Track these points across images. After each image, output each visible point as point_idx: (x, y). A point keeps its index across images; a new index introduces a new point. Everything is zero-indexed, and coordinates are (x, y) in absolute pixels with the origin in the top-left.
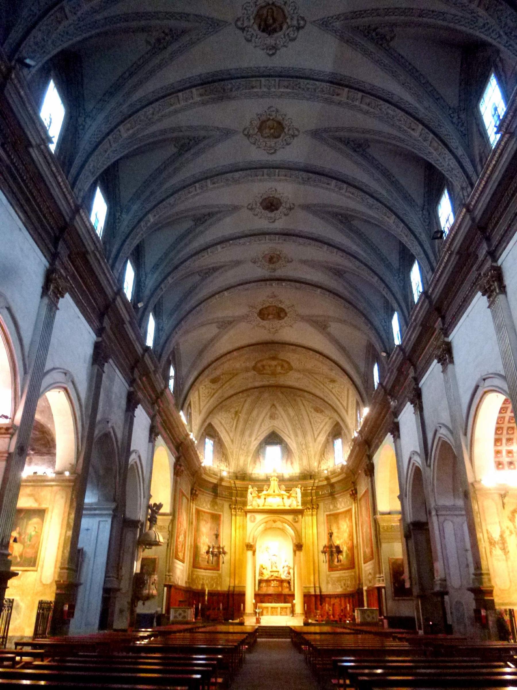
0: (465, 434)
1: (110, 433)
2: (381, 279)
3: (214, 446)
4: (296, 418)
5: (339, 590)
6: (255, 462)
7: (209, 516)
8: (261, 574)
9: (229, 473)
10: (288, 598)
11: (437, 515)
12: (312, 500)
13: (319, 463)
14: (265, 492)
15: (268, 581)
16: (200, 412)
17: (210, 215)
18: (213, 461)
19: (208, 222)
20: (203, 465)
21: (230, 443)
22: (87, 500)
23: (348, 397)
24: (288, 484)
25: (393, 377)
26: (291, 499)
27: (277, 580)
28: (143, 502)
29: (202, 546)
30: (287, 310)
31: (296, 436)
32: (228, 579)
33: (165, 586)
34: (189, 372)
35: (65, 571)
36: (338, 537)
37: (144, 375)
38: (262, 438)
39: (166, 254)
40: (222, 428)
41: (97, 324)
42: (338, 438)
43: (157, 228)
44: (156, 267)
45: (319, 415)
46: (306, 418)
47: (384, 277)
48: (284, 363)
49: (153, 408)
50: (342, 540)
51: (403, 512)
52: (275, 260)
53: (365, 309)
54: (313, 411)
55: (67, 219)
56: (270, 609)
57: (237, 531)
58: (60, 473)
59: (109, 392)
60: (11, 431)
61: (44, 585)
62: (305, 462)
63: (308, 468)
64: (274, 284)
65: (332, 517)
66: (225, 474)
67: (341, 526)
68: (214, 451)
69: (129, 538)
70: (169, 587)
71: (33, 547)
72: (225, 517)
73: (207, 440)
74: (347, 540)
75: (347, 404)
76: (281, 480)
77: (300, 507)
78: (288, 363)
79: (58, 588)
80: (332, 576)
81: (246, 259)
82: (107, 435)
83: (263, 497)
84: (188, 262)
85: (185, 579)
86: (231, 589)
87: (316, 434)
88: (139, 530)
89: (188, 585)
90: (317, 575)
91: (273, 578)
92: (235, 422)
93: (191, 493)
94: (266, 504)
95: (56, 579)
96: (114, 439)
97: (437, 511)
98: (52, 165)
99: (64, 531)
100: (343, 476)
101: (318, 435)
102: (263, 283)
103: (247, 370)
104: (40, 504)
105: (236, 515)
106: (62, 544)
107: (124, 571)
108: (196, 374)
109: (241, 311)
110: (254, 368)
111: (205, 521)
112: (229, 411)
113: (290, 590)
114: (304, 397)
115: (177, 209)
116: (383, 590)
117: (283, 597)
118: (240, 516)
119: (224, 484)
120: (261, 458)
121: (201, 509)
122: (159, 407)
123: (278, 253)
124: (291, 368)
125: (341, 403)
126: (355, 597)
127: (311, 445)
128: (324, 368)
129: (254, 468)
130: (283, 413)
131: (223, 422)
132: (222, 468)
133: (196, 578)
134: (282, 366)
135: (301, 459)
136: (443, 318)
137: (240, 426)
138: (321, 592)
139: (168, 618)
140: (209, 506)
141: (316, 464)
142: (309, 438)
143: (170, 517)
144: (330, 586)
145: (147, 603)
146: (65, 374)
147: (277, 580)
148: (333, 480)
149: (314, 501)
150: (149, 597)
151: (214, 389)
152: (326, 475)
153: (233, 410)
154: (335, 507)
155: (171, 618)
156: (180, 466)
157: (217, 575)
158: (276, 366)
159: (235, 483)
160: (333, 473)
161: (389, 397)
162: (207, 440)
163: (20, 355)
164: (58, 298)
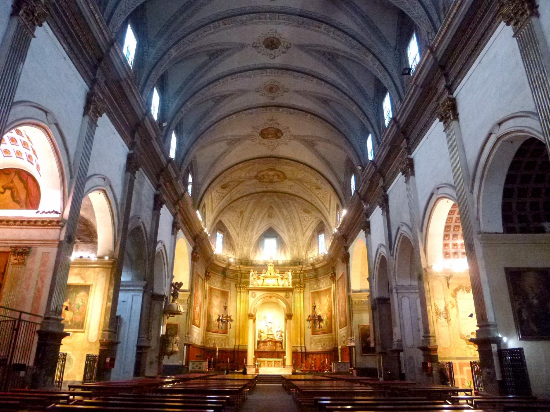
0: (421, 231)
1: (140, 227)
2: (359, 106)
3: (223, 238)
4: (289, 217)
5: (320, 349)
6: (256, 252)
8: (260, 336)
9: (235, 259)
10: (280, 354)
11: (397, 293)
12: (300, 281)
13: (307, 253)
14: (263, 275)
15: (265, 342)
16: (213, 211)
17: (222, 51)
18: (223, 250)
19: (219, 58)
20: (214, 253)
21: (236, 235)
22: (123, 279)
23: (330, 201)
24: (281, 268)
25: (367, 186)
26: (284, 280)
27: (272, 341)
28: (167, 281)
29: (213, 315)
30: (283, 131)
31: (289, 231)
32: (234, 340)
33: (185, 345)
34: (204, 179)
35: (107, 333)
36: (320, 309)
37: (167, 182)
38: (261, 233)
39: (185, 84)
41: (129, 139)
42: (321, 234)
43: (178, 61)
44: (178, 92)
45: (307, 215)
46: (296, 216)
47: (362, 106)
48: (280, 174)
49: (175, 207)
50: (323, 312)
51: (371, 291)
52: (274, 90)
53: (345, 131)
54: (302, 212)
55: (104, 51)
56: (266, 362)
57: (241, 304)
58: (101, 258)
59: (139, 194)
60: (61, 223)
61: (90, 343)
62: (295, 252)
63: (297, 257)
64: (273, 109)
65: (316, 294)
66: (232, 260)
67: (322, 301)
68: (223, 243)
69: (157, 308)
70: (188, 346)
71: (80, 314)
72: (232, 294)
73: (218, 234)
74: (327, 311)
75: (330, 207)
76: (276, 265)
77: (291, 287)
78: (284, 174)
79: (102, 345)
80: (314, 338)
81: (250, 89)
82: (138, 229)
83: (262, 278)
84: (203, 90)
85: (201, 339)
86: (237, 347)
87: (304, 229)
88: (164, 302)
89: (203, 345)
90: (303, 338)
92: (240, 220)
93: (206, 275)
94: (264, 284)
95: (100, 338)
96: (144, 232)
97: (397, 290)
98: (90, 4)
99: (105, 303)
100: (325, 262)
101: (306, 231)
102: (264, 109)
103: (250, 178)
104: (85, 281)
105: (240, 292)
106: (104, 312)
107: (153, 332)
108: (209, 181)
109: (247, 131)
110: (256, 177)
112: (236, 212)
113: (282, 348)
114: (296, 200)
115: (194, 45)
116: (354, 348)
117: (276, 354)
118: (244, 292)
119: (231, 268)
120: (261, 249)
121: (213, 287)
122: (180, 206)
123: (277, 84)
124: (285, 178)
125: (325, 206)
126: (332, 354)
127: (300, 238)
128: (312, 178)
129: (255, 256)
130: (278, 213)
131: (231, 219)
132: (229, 256)
134: (278, 176)
135: (292, 250)
136: (408, 139)
137: (244, 223)
138: (305, 350)
139: (188, 369)
141: (304, 253)
142: (299, 233)
143: (189, 293)
144: (313, 345)
145: (171, 357)
146: (104, 179)
147: (272, 341)
148: (317, 266)
149: (302, 282)
150: (173, 353)
151: (223, 193)
152: (312, 262)
154: (318, 286)
155: (190, 369)
156: (197, 253)
158: (273, 175)
159: (240, 268)
160: (317, 260)
161: (362, 202)
162: (218, 234)
163: (66, 162)
164: (97, 117)
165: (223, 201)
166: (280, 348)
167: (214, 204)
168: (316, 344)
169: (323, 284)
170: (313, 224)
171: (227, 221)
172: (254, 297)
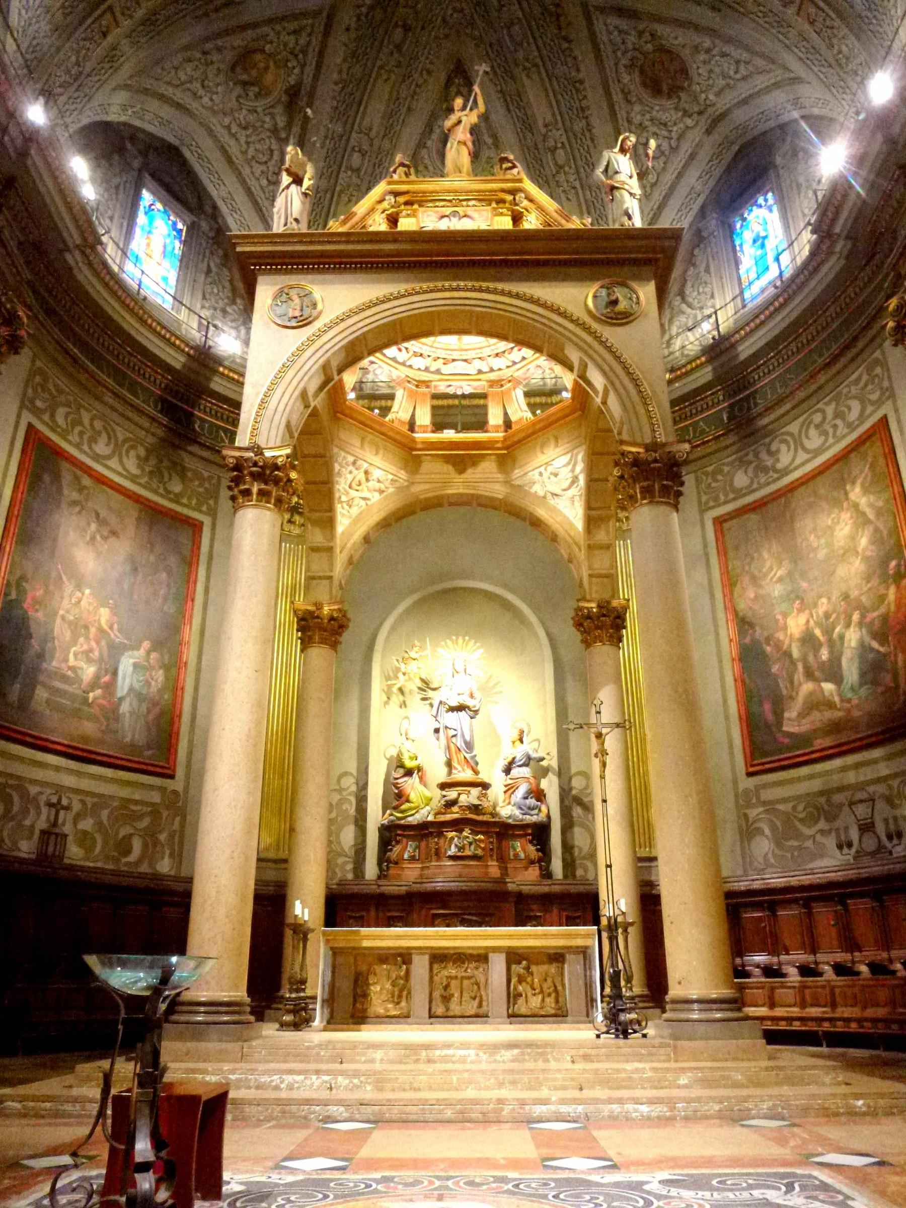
4: (558, 135)
7: (133, 511)
8: (396, 797)
15: (424, 831)
27: (477, 826)
29: (61, 631)
40: (230, 180)
56: (420, 966)
91: (455, 814)
113: (547, 874)
131: (234, 149)
140: (132, 465)
144: (763, 846)
148: (745, 350)
153: (277, 81)
157: (156, 797)
166: (533, 873)
168: (785, 832)
169: (799, 444)
170: (692, 178)
171: (215, 156)
172: (303, 322)
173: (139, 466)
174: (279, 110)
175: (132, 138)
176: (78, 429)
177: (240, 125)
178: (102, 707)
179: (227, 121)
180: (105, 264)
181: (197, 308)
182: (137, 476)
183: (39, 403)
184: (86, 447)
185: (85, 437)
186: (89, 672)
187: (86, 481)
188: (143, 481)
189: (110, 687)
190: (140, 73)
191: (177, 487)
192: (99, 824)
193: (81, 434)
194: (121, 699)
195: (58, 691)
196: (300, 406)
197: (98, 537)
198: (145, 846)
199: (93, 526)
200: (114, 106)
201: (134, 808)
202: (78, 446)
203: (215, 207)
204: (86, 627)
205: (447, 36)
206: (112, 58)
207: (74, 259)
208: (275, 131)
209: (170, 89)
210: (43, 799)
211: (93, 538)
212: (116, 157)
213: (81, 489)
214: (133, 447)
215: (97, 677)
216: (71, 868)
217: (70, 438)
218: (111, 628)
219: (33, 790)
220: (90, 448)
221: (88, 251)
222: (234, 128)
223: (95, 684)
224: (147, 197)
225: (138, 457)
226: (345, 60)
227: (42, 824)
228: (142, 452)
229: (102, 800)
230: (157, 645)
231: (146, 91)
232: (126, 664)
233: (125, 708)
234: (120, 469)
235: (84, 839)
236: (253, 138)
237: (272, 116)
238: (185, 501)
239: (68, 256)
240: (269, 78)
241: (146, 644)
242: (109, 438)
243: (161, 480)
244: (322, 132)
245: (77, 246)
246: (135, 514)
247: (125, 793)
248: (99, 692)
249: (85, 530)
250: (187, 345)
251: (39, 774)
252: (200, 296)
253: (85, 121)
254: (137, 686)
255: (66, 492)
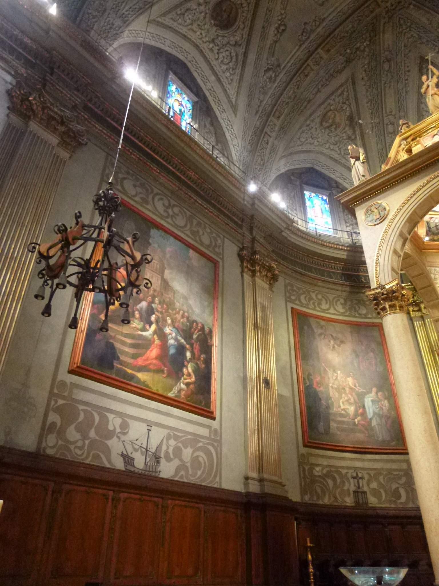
7: (348, 329)
16: (234, 108)
29: (333, 394)
89: (254, 488)
111: (335, 339)
131: (336, 156)
133: (329, 475)
151: (236, 44)
153: (341, 118)
165: (249, 69)
167: (227, 86)
172: (382, 219)
173: (343, 308)
174: (347, 128)
175: (293, 174)
176: (312, 302)
177: (334, 144)
178: (363, 425)
179: (327, 146)
180: (299, 230)
181: (345, 229)
182: (344, 313)
183: (293, 298)
184: (317, 308)
185: (316, 304)
186: (351, 409)
187: (322, 323)
188: (347, 314)
189: (364, 414)
190: (285, 150)
191: (364, 311)
192: (380, 484)
193: (314, 304)
194: (371, 419)
195: (339, 422)
196: (396, 258)
197: (336, 346)
198: (407, 492)
199: (332, 342)
200: (281, 166)
201: (396, 473)
202: (314, 309)
203: (336, 182)
204: (344, 389)
205: (410, 51)
206: (273, 150)
207: (286, 234)
208: (349, 138)
209: (300, 147)
210: (349, 476)
211: (334, 347)
212: (289, 185)
213: (322, 327)
214: (338, 300)
215: (356, 411)
216: (374, 509)
217: (310, 307)
218: (355, 386)
219: (344, 471)
220: (320, 308)
221: (290, 228)
222: (332, 147)
223: (356, 415)
224: (307, 193)
225: (341, 304)
226: (367, 91)
227: (353, 488)
228: (342, 301)
229: (378, 472)
230: (380, 389)
231: (291, 154)
232: (368, 401)
233: (374, 423)
234: (336, 312)
235: (376, 493)
236: (341, 146)
237: (345, 132)
238: (370, 316)
239: (283, 233)
240: (337, 119)
241: (374, 390)
242: (326, 300)
243: (356, 311)
244: (370, 126)
245: (286, 228)
246: (349, 330)
247: (388, 466)
248: (359, 418)
249: (329, 345)
250: (345, 246)
251: (344, 464)
252: (344, 223)
253: (273, 178)
254: (377, 411)
255: (315, 331)
